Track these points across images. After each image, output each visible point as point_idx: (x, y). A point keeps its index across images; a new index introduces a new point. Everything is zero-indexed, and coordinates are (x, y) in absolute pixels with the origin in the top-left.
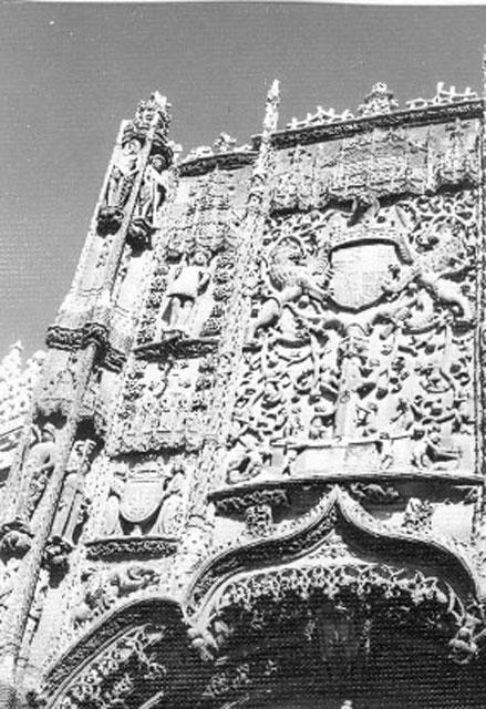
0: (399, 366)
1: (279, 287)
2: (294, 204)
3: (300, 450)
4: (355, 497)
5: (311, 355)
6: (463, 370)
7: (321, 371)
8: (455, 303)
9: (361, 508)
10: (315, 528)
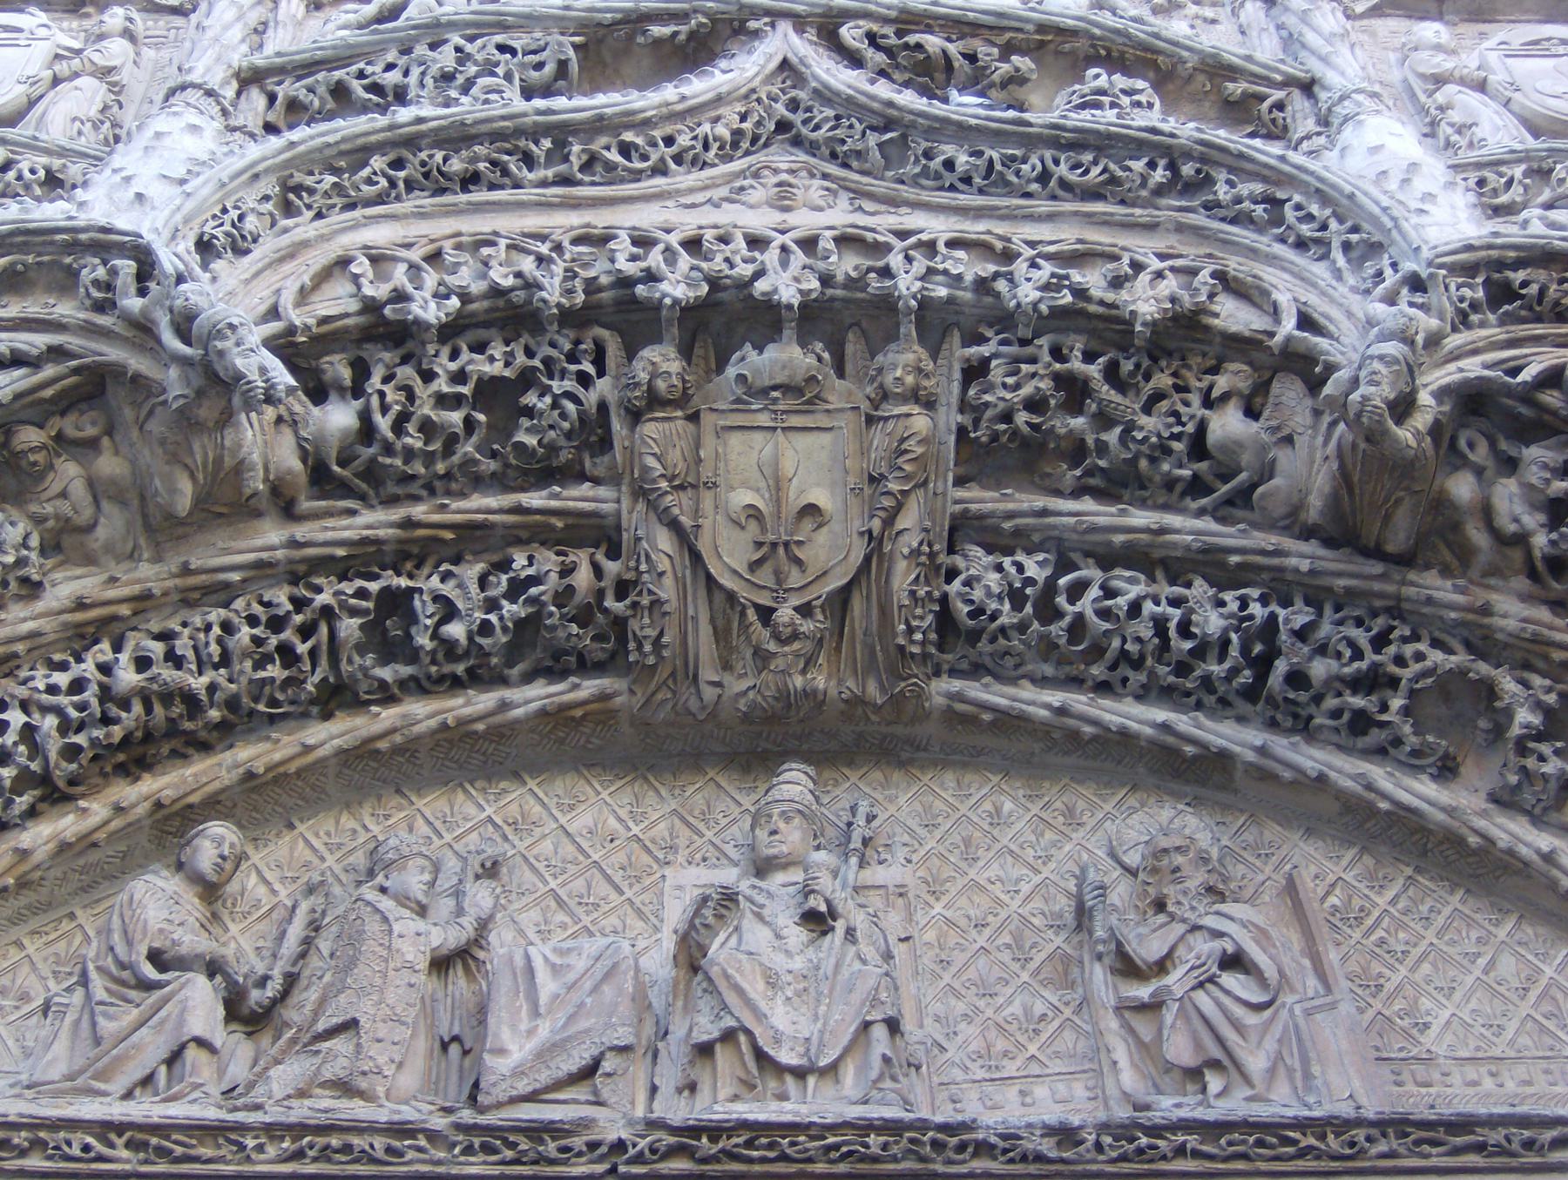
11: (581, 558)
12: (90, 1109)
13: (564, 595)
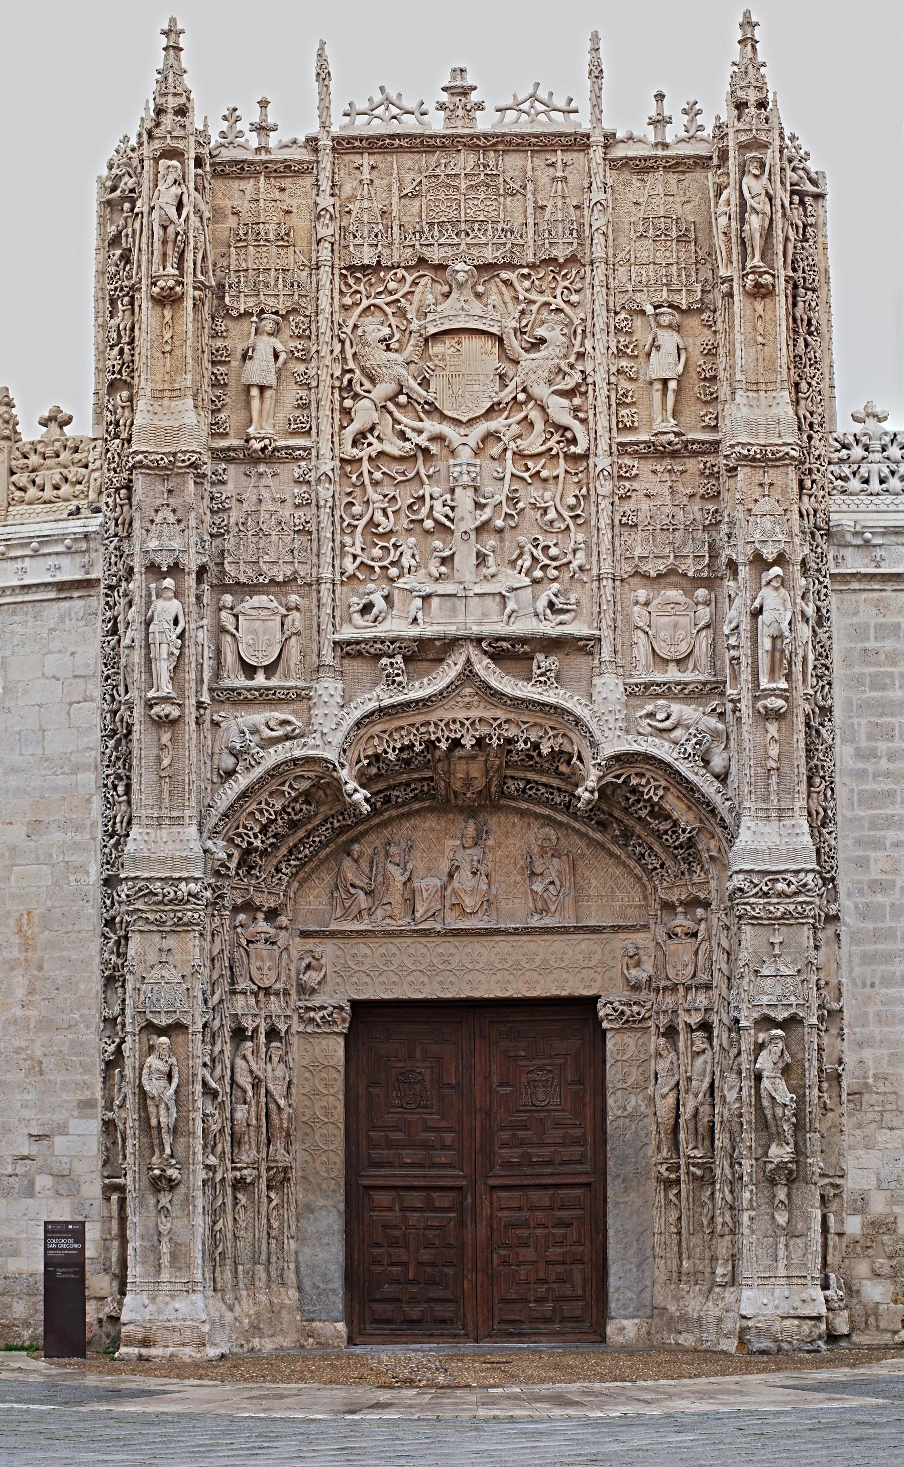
0: (513, 500)
1: (372, 380)
2: (374, 262)
3: (426, 598)
4: (485, 653)
5: (418, 473)
6: (579, 512)
7: (432, 498)
8: (567, 429)
9: (493, 666)
10: (452, 683)
11: (425, 783)
12: (348, 926)
13: (422, 791)
